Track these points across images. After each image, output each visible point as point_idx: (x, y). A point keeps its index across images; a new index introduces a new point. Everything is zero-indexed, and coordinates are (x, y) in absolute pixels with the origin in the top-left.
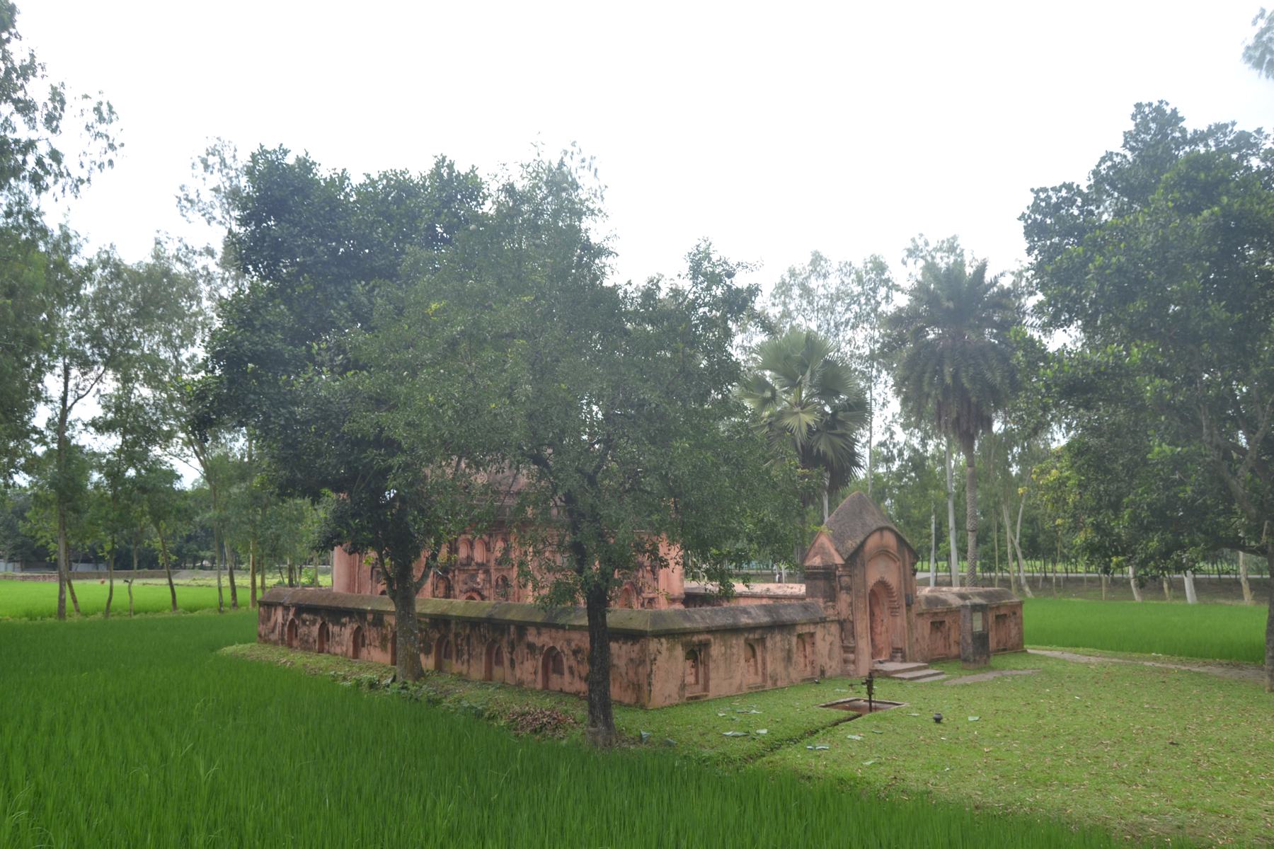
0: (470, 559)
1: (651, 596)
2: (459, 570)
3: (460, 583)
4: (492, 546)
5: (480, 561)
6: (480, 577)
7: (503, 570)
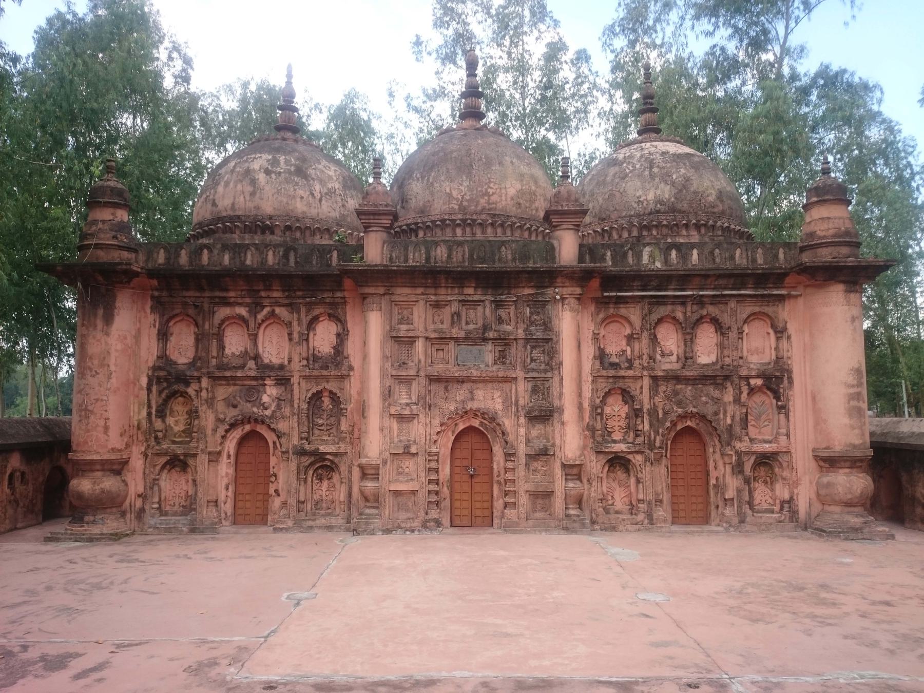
1: (767, 448)
2: (213, 378)
3: (220, 406)
5: (276, 361)
6: (270, 393)
7: (327, 379)
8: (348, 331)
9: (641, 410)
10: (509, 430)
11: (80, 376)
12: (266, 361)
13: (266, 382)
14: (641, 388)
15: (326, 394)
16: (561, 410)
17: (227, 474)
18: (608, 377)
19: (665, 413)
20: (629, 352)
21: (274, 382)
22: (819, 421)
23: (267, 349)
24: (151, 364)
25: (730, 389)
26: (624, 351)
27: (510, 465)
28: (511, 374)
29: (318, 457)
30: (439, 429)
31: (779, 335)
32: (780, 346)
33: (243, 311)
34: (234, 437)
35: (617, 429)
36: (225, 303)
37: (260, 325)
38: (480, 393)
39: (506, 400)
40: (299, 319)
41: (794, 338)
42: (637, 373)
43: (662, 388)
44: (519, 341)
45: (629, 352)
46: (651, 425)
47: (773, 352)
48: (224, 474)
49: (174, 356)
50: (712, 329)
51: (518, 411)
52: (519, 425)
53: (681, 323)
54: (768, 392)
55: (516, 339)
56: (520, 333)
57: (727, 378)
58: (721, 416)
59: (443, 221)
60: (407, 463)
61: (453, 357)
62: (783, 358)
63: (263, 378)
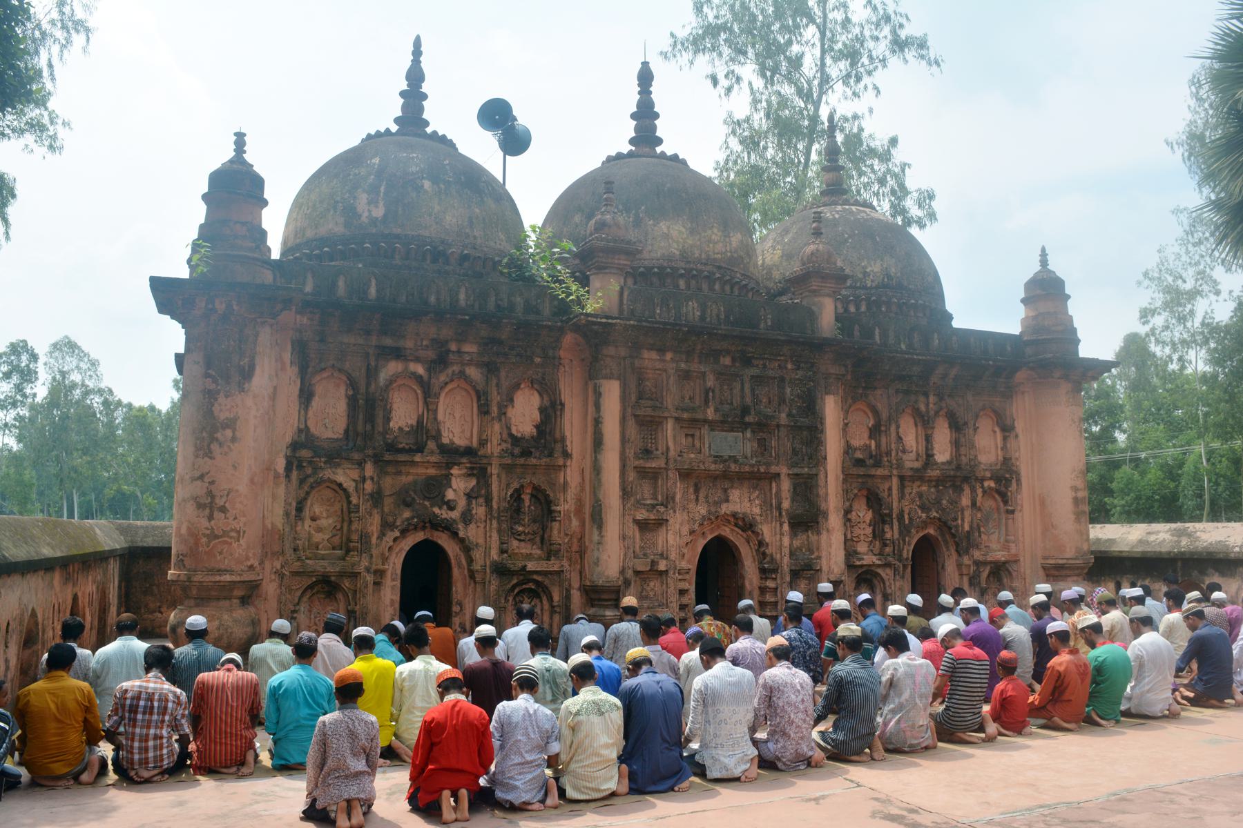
0: (423, 433)
4: (495, 398)
5: (460, 442)
6: (459, 485)
8: (562, 405)
9: (890, 515)
10: (767, 540)
11: (201, 453)
12: (445, 441)
13: (453, 471)
14: (890, 489)
15: (529, 491)
16: (825, 515)
17: (392, 600)
18: (859, 476)
19: (910, 519)
20: (873, 447)
21: (464, 471)
22: (1048, 527)
23: (448, 425)
24: (288, 439)
25: (967, 491)
26: (868, 447)
27: (771, 584)
28: (774, 469)
29: (522, 578)
30: (689, 539)
31: (1007, 434)
32: (1008, 446)
33: (420, 370)
34: (401, 550)
35: (862, 538)
36: (398, 354)
37: (442, 388)
38: (735, 494)
39: (766, 505)
40: (497, 385)
41: (1021, 436)
42: (886, 472)
43: (907, 490)
44: (782, 429)
45: (873, 447)
46: (901, 533)
47: (1000, 452)
48: (387, 602)
49: (316, 430)
50: (946, 425)
51: (780, 514)
52: (782, 534)
53: (923, 416)
54: (997, 496)
55: (778, 426)
56: (783, 418)
57: (966, 479)
58: (960, 522)
59: (662, 268)
60: (652, 584)
61: (707, 446)
62: (1011, 459)
63: (449, 466)
